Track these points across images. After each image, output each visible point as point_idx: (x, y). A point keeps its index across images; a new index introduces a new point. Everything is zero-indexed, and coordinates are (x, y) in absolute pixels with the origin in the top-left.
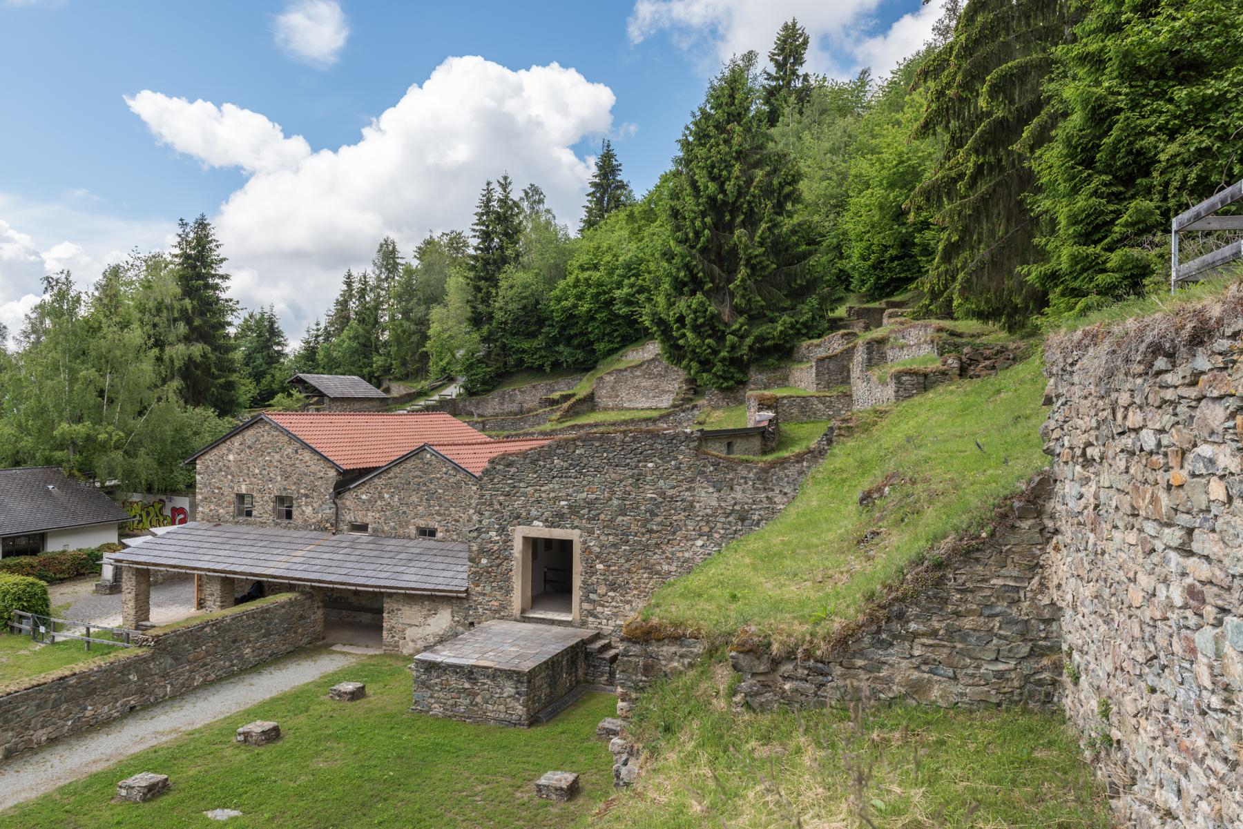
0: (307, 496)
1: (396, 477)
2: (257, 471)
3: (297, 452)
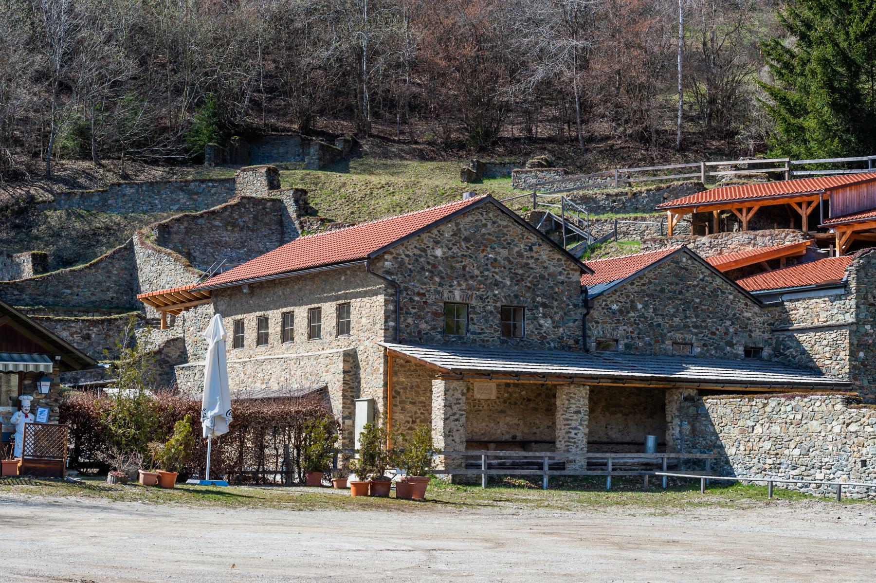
0: (544, 305)
1: (650, 283)
2: (477, 272)
3: (531, 249)
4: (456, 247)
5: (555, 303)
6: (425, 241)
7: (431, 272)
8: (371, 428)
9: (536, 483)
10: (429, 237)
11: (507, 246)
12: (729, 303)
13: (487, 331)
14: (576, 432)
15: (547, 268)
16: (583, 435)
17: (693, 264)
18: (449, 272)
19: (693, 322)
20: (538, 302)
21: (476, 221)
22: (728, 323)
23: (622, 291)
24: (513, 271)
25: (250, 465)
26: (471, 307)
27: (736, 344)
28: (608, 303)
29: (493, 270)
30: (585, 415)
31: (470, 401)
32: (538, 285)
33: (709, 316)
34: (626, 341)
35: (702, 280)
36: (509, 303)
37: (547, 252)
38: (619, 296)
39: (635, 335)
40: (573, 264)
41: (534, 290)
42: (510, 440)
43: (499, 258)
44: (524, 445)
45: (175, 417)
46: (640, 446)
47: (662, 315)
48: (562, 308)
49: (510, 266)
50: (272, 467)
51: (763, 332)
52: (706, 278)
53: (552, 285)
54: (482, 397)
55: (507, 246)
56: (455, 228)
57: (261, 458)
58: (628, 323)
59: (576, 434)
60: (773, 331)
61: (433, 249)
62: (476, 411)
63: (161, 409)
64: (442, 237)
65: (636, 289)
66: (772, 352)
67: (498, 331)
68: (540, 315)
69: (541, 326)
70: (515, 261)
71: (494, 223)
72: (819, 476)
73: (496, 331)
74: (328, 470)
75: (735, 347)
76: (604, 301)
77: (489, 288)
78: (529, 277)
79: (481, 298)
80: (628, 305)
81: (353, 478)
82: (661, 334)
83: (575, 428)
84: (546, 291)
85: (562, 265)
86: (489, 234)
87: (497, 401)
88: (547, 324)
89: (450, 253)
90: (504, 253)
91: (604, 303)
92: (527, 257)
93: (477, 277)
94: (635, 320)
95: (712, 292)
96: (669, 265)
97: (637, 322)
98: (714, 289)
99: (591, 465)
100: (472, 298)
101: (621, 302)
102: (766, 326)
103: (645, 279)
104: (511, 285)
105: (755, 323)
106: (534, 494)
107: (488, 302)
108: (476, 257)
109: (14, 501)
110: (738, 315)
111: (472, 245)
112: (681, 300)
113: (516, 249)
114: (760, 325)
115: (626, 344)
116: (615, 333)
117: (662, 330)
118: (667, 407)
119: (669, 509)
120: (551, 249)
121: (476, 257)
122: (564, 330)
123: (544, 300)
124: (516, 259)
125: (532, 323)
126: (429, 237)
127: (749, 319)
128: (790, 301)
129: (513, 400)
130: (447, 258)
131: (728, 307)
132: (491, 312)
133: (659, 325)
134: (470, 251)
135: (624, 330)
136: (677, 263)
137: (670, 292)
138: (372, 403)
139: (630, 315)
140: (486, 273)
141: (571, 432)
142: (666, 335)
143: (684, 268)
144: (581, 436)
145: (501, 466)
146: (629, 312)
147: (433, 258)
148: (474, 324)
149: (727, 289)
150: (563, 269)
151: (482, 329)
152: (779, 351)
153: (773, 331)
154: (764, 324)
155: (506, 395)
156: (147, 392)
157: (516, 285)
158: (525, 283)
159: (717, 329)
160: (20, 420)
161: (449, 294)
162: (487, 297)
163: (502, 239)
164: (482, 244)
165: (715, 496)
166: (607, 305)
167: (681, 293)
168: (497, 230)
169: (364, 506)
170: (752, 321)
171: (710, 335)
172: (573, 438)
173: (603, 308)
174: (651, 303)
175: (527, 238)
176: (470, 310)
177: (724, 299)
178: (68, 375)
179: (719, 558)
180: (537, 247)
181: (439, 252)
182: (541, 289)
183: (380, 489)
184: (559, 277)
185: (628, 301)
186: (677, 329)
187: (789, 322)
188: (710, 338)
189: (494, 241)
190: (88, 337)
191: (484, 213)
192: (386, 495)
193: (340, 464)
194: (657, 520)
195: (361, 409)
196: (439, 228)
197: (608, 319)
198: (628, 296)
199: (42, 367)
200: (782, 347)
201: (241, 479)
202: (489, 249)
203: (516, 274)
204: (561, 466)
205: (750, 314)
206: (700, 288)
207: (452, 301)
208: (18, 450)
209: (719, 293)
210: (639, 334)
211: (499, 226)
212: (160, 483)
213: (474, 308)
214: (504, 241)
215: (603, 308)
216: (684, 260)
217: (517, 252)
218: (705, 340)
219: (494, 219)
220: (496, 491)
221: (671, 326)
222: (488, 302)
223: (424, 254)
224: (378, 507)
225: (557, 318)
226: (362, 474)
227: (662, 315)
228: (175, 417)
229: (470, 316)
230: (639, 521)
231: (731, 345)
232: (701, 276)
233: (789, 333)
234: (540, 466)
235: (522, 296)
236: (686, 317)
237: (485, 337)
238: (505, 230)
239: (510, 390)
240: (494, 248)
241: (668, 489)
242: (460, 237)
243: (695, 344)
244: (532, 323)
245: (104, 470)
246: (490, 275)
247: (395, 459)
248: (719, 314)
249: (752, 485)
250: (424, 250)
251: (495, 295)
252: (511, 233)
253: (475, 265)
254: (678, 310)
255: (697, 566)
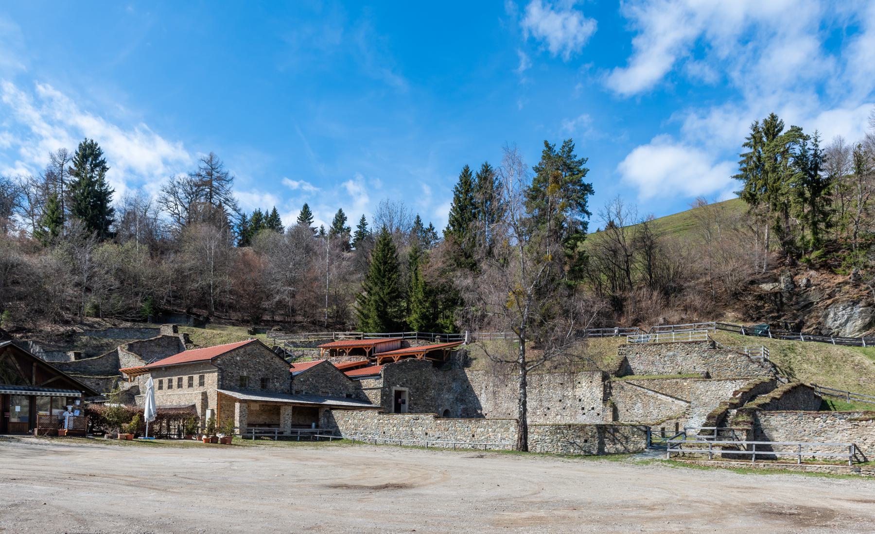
0: (277, 378)
2: (252, 366)
8: (212, 419)
9: (273, 438)
25: (164, 432)
44: (269, 425)
45: (133, 414)
46: (310, 426)
50: (173, 433)
57: (169, 430)
63: (128, 411)
72: (370, 437)
74: (195, 434)
81: (204, 437)
88: (278, 384)
89: (242, 359)
90: (263, 360)
99: (292, 432)
106: (272, 442)
109: (63, 445)
119: (319, 447)
138: (212, 411)
144: (289, 422)
145: (260, 433)
156: (122, 405)
160: (67, 414)
164: (254, 356)
165: (335, 443)
169: (208, 447)
178: (90, 398)
179: (334, 464)
181: (238, 358)
183: (214, 440)
186: (323, 388)
187: (362, 387)
190: (98, 384)
192: (217, 443)
193: (200, 432)
194: (314, 451)
195: (208, 413)
199: (76, 395)
201: (161, 437)
204: (282, 433)
208: (66, 426)
212: (127, 438)
220: (258, 441)
224: (213, 447)
225: (281, 382)
226: (207, 435)
228: (133, 414)
230: (308, 451)
234: (274, 433)
241: (319, 440)
245: (104, 433)
247: (220, 430)
249: (347, 440)
250: (233, 358)
255: (326, 466)
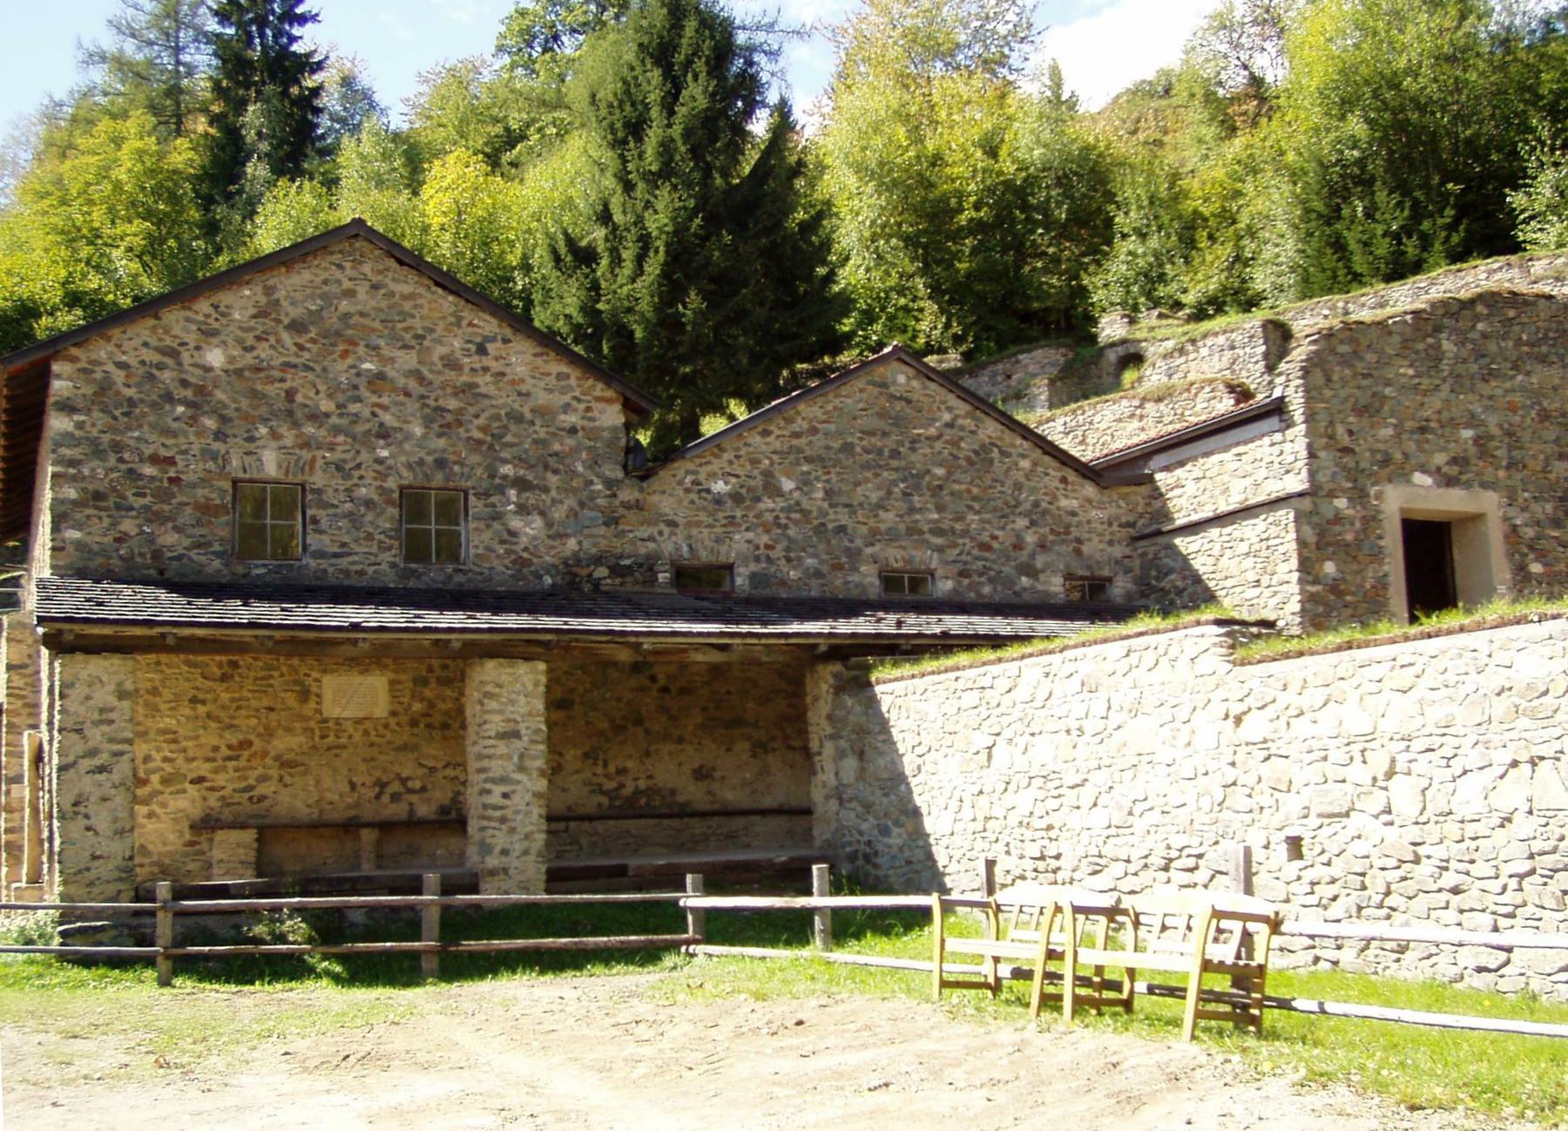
0: (522, 484)
1: (814, 431)
2: (326, 405)
3: (482, 350)
4: (264, 345)
5: (553, 480)
6: (176, 331)
7: (189, 404)
10: (188, 320)
11: (413, 342)
12: (1020, 477)
13: (358, 549)
14: (506, 789)
15: (528, 394)
16: (528, 797)
17: (925, 388)
18: (245, 403)
19: (930, 522)
20: (505, 477)
21: (325, 282)
22: (1022, 523)
23: (738, 449)
24: (431, 402)
26: (314, 491)
27: (1043, 571)
28: (702, 477)
29: (374, 399)
30: (533, 742)
31: (312, 724)
32: (501, 437)
33: (970, 508)
34: (753, 567)
35: (950, 425)
36: (420, 481)
37: (528, 358)
38: (731, 462)
39: (778, 552)
40: (600, 386)
41: (491, 447)
42: (433, 817)
43: (390, 372)
47: (847, 506)
48: (574, 491)
49: (422, 390)
51: (1111, 543)
52: (960, 422)
53: (542, 435)
54: (344, 715)
55: (413, 342)
56: (263, 300)
58: (758, 525)
59: (505, 796)
60: (1135, 539)
61: (198, 348)
62: (329, 749)
64: (224, 321)
65: (778, 445)
66: (1134, 588)
67: (390, 548)
68: (512, 507)
69: (513, 533)
70: (438, 380)
71: (375, 287)
73: (383, 548)
75: (1042, 577)
76: (688, 472)
77: (363, 444)
78: (477, 416)
79: (339, 468)
80: (758, 482)
82: (848, 550)
83: (503, 780)
84: (526, 451)
85: (570, 388)
86: (362, 314)
87: (392, 721)
88: (530, 529)
89: (249, 359)
90: (408, 360)
91: (689, 479)
92: (472, 370)
93: (327, 415)
94: (777, 517)
95: (975, 452)
96: (861, 391)
97: (783, 521)
98: (983, 446)
100: (312, 468)
101: (737, 476)
102: (1115, 528)
103: (799, 421)
104: (424, 436)
105: (1089, 522)
107: (361, 478)
108: (324, 370)
110: (1044, 505)
111: (313, 341)
112: (896, 470)
113: (442, 350)
114: (1100, 528)
115: (753, 576)
116: (724, 549)
117: (851, 541)
118: (810, 714)
120: (539, 350)
121: (324, 370)
122: (580, 543)
123: (522, 472)
124: (439, 373)
125: (488, 526)
126: (188, 320)
127: (1074, 514)
128: (1167, 469)
129: (437, 719)
130: (239, 373)
131: (1018, 486)
132: (369, 504)
133: (842, 529)
134: (306, 355)
135: (749, 542)
136: (884, 385)
137: (867, 452)
139: (761, 506)
140: (354, 408)
141: (489, 792)
142: (859, 552)
143: (900, 398)
146: (758, 500)
147: (199, 372)
148: (321, 532)
149: (1013, 445)
150: (575, 398)
151: (343, 545)
152: (1148, 584)
153: (1135, 539)
154: (1110, 524)
155: (417, 707)
157: (440, 435)
158: (467, 431)
159: (994, 538)
161: (247, 459)
162: (359, 466)
163: (400, 326)
164: (341, 338)
166: (699, 484)
167: (895, 454)
168: (383, 304)
170: (1082, 517)
171: (976, 552)
172: (495, 808)
173: (687, 491)
174: (817, 479)
175: (470, 324)
176: (309, 497)
177: (1008, 470)
180: (499, 344)
181: (215, 358)
182: (512, 445)
184: (563, 417)
185: (756, 472)
186: (892, 537)
187: (1166, 515)
188: (977, 558)
189: (374, 330)
191: (348, 265)
196: (214, 300)
197: (703, 517)
198: (755, 462)
200: (1154, 573)
202: (361, 350)
203: (440, 410)
205: (1075, 503)
206: (947, 442)
207: (256, 476)
209: (995, 454)
210: (788, 549)
211: (392, 294)
213: (318, 492)
214: (406, 330)
215: (687, 491)
216: (901, 379)
217: (442, 358)
218: (965, 563)
219: (376, 279)
221: (874, 532)
222: (361, 478)
223: (169, 361)
225: (558, 514)
227: (847, 506)
229: (309, 512)
231: (1031, 571)
232: (947, 417)
233: (1162, 540)
235: (455, 463)
236: (912, 510)
237: (353, 563)
238: (408, 306)
239: (428, 693)
240: (376, 348)
242: (278, 321)
243: (939, 573)
244: (488, 526)
246: (366, 412)
248: (999, 503)
250: (173, 353)
251: (380, 461)
252: (425, 312)
253: (322, 388)
254: (889, 493)
